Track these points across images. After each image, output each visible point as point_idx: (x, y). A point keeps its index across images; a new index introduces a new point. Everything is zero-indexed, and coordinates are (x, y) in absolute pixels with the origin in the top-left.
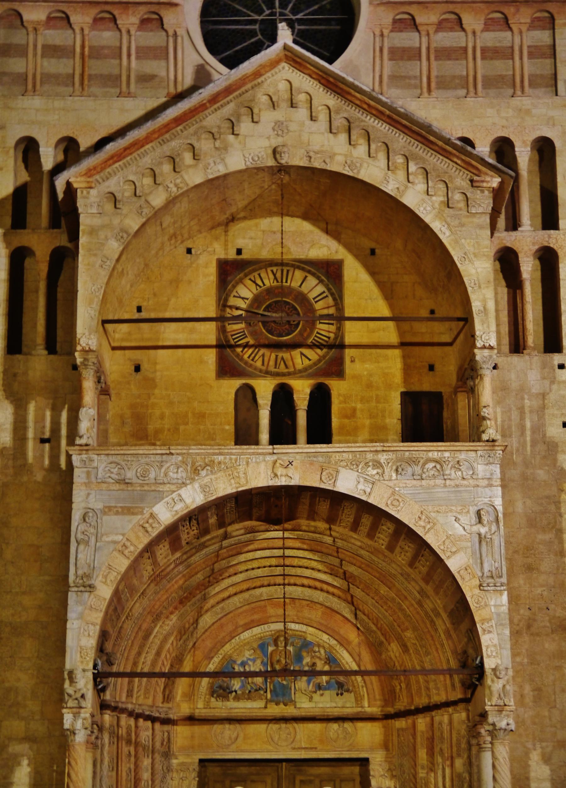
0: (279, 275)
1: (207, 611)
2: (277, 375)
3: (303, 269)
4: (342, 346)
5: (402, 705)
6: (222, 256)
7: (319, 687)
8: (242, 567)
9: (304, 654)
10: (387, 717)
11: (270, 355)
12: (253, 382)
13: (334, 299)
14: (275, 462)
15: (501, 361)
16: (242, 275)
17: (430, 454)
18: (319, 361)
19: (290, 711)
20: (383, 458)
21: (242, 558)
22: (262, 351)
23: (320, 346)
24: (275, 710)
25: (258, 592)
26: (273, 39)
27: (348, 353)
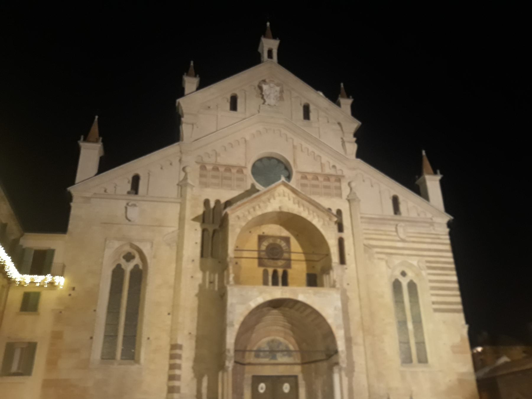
24: (273, 361)
26: (280, 179)
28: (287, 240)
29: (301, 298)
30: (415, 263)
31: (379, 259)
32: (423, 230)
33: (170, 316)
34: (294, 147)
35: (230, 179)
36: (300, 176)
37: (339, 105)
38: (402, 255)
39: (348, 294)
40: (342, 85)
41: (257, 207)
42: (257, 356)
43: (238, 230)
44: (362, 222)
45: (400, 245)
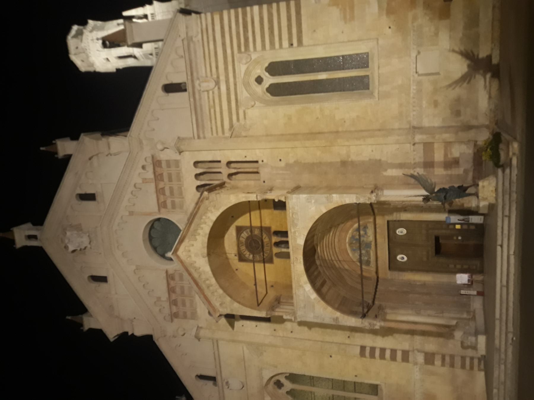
0: (242, 245)
1: (344, 267)
2: (271, 248)
3: (239, 237)
4: (261, 227)
5: (370, 210)
6: (237, 261)
7: (366, 234)
8: (330, 258)
9: (355, 238)
10: (374, 214)
11: (266, 248)
12: (274, 254)
13: (247, 229)
14: (296, 263)
15: (262, 180)
16: (242, 255)
17: (291, 216)
18: (267, 234)
19: (373, 244)
20: (293, 231)
21: (327, 258)
22: (265, 249)
23: (262, 234)
25: (337, 251)
27: (263, 225)
28: (239, 230)
29: (301, 242)
30: (243, 68)
31: (245, 118)
32: (200, 53)
33: (333, 356)
34: (131, 213)
35: (182, 288)
36: (163, 210)
37: (68, 158)
38: (235, 84)
39: (291, 161)
40: (42, 149)
41: (207, 282)
42: (368, 263)
43: (236, 305)
44: (204, 138)
45: (223, 87)
